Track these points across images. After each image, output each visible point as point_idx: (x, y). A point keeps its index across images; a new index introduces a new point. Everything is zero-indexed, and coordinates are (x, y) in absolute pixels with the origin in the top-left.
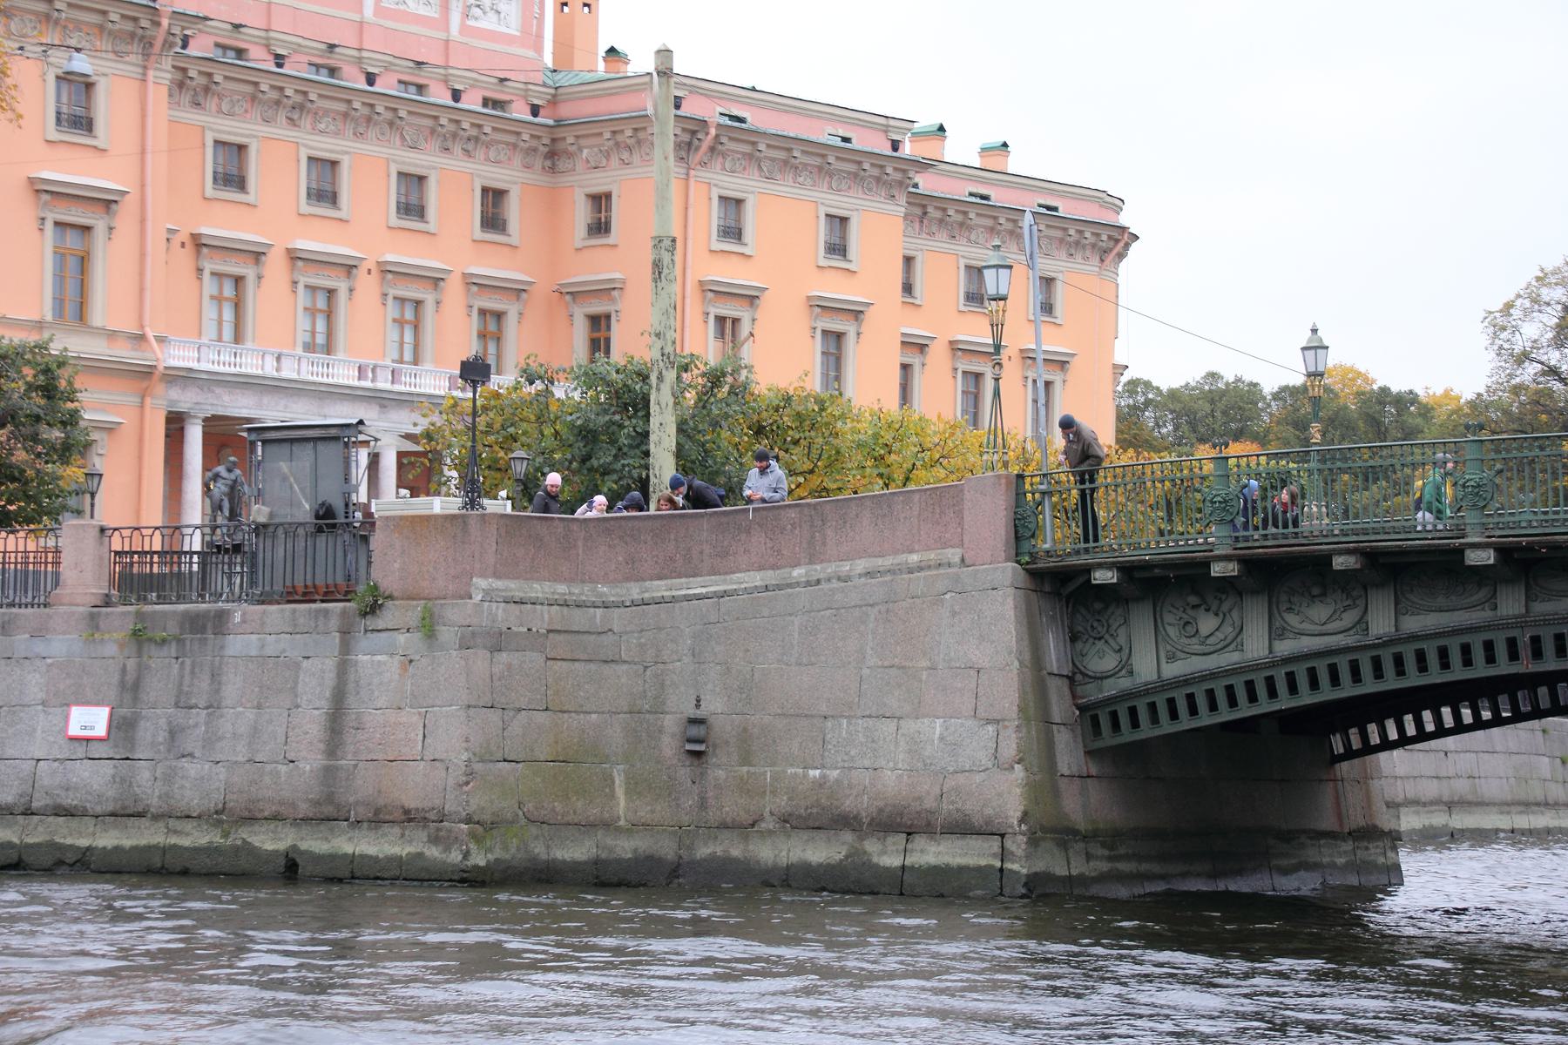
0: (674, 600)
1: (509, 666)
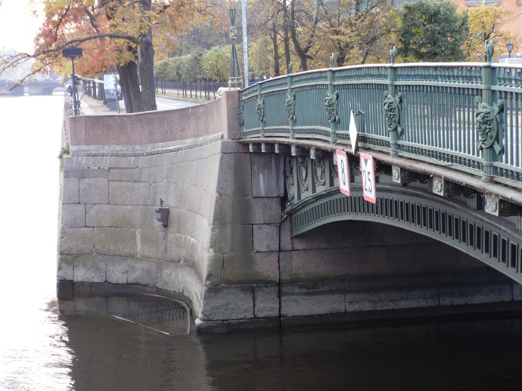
0: (162, 152)
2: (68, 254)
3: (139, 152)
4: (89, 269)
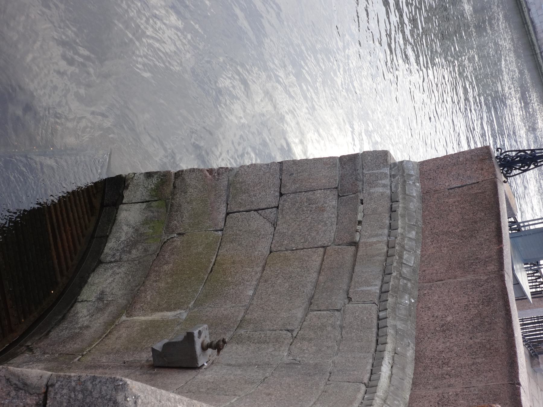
1: (322, 210)
2: (175, 187)
3: (390, 300)
4: (136, 230)
